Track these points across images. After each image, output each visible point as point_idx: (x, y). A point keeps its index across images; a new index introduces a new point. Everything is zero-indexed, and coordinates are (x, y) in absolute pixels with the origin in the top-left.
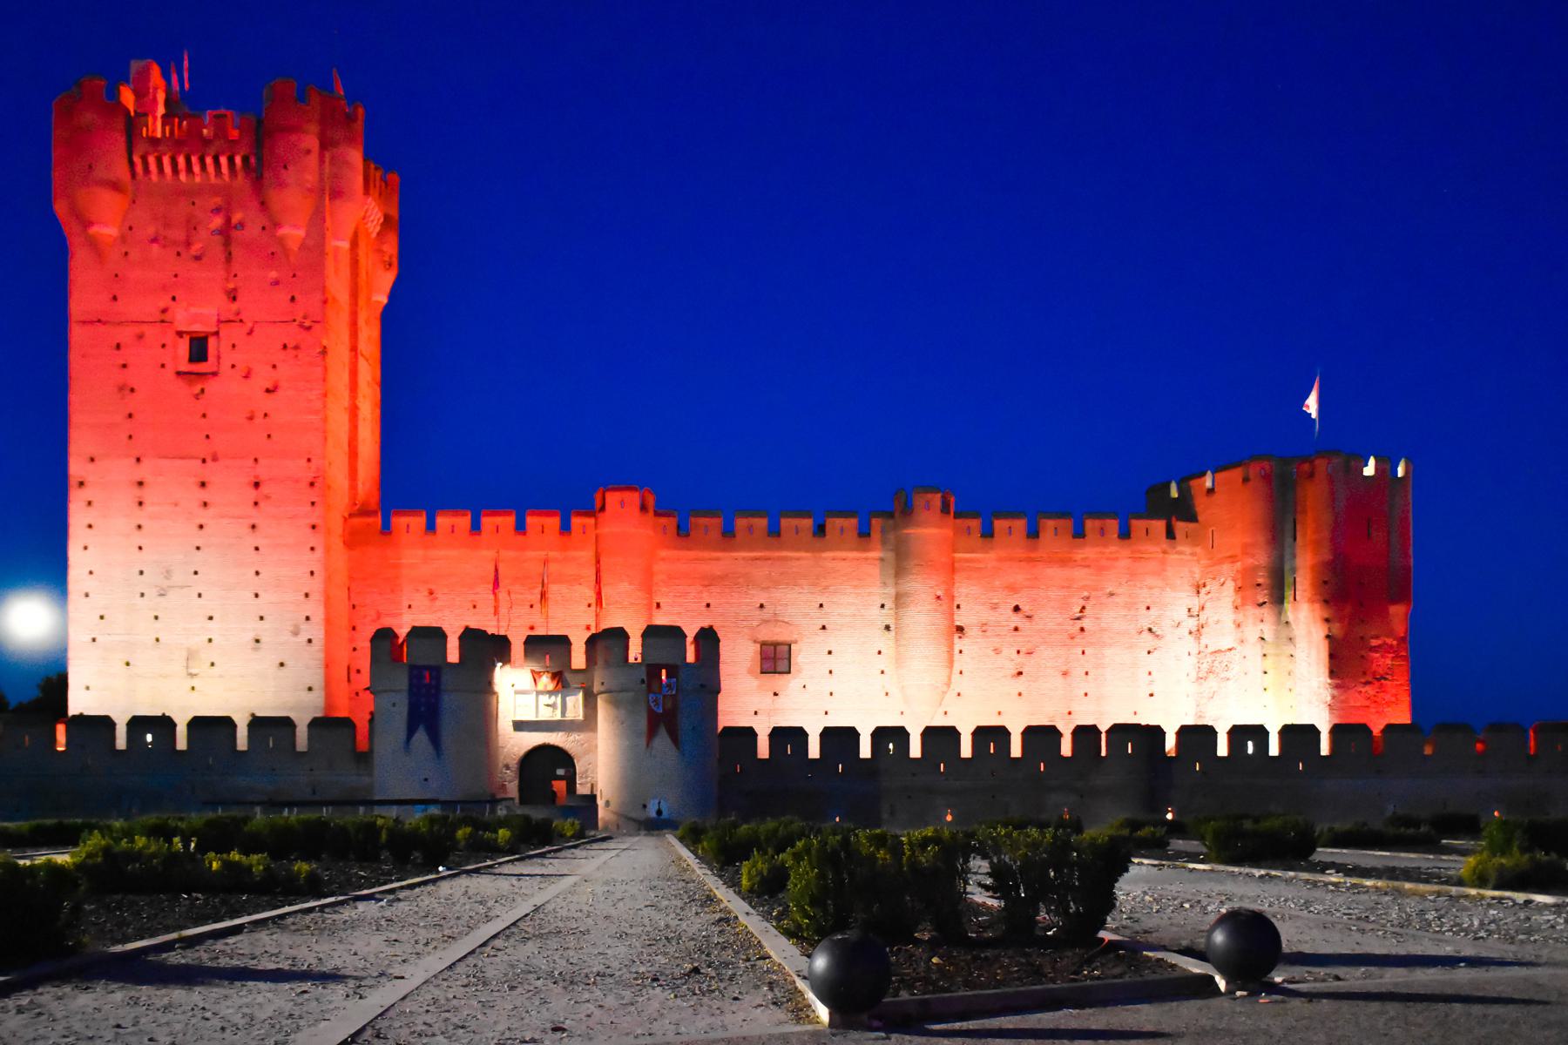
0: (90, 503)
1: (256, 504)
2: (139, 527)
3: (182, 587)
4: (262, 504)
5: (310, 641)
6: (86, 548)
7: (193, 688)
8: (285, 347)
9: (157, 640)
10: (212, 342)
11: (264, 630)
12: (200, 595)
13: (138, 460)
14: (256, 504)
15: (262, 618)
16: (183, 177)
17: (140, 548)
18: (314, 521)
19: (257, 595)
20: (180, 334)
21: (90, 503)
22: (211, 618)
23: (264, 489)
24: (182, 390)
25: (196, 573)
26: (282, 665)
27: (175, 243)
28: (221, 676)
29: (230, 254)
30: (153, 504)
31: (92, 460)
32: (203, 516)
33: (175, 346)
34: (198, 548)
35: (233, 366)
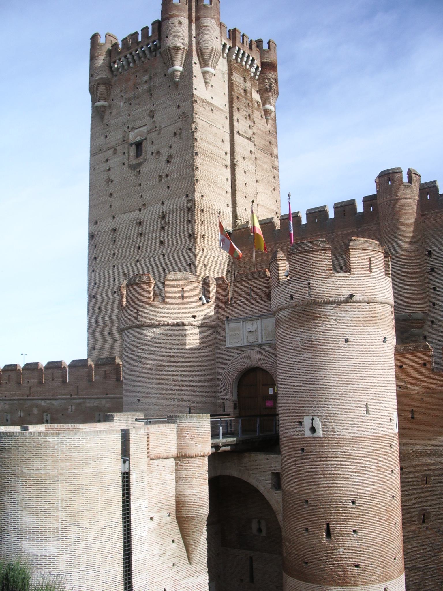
1: (163, 228)
4: (166, 228)
8: (175, 134)
13: (114, 217)
14: (163, 228)
20: (131, 145)
23: (167, 219)
24: (130, 174)
29: (151, 95)
33: (128, 152)
34: (138, 261)
35: (152, 153)
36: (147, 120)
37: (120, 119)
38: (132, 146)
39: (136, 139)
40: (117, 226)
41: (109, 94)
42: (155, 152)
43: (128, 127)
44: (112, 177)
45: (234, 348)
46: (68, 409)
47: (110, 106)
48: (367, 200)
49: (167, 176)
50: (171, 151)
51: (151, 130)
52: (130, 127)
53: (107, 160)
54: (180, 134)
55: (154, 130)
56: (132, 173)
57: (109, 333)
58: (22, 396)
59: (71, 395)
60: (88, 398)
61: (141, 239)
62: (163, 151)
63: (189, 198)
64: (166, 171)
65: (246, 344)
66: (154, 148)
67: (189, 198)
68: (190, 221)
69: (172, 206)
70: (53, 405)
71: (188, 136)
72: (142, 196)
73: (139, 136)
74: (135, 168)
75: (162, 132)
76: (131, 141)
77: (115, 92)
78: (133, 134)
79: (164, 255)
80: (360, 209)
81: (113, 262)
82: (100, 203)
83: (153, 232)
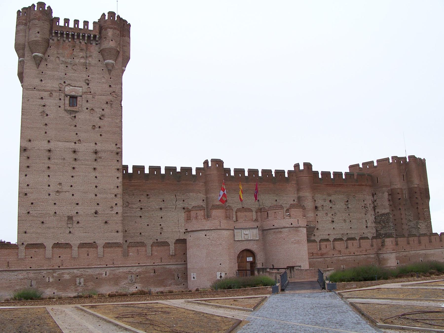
0: (28, 158)
1: (96, 160)
2: (49, 167)
3: (66, 192)
5: (117, 213)
6: (26, 175)
7: (70, 232)
9: (55, 213)
10: (79, 99)
11: (98, 208)
12: (73, 195)
13: (49, 141)
15: (98, 204)
16: (70, 40)
17: (49, 176)
18: (119, 167)
19: (96, 195)
20: (67, 96)
21: (28, 158)
22: (77, 204)
23: (100, 155)
24: (68, 117)
25: (71, 186)
26: (106, 222)
27: (66, 63)
28: (81, 227)
30: (54, 159)
31: (30, 141)
32: (76, 164)
34: (72, 177)
35: (87, 109)
36: (83, 84)
37: (56, 73)
38: (67, 97)
39: (72, 93)
40: (53, 149)
41: (46, 50)
42: (89, 109)
43: (65, 82)
44: (48, 112)
45: (238, 241)
46: (102, 274)
47: (46, 60)
48: (198, 169)
49: (100, 127)
50: (103, 113)
51: (86, 92)
52: (67, 83)
53: (42, 98)
54: (111, 104)
55: (89, 94)
56: (67, 115)
57: (43, 222)
58: (53, 267)
59: (107, 265)
60: (120, 267)
61: (76, 163)
62: (96, 110)
63: (118, 146)
64: (99, 124)
65: (243, 239)
66: (88, 105)
67: (118, 146)
68: (118, 161)
69: (104, 148)
70: (87, 272)
71: (117, 108)
72: (77, 134)
73: (74, 92)
74: (73, 113)
75: (96, 97)
76: (67, 93)
77: (52, 51)
78: (69, 88)
79: (96, 177)
80: (194, 173)
81: (49, 174)
82: (35, 127)
83: (87, 160)
